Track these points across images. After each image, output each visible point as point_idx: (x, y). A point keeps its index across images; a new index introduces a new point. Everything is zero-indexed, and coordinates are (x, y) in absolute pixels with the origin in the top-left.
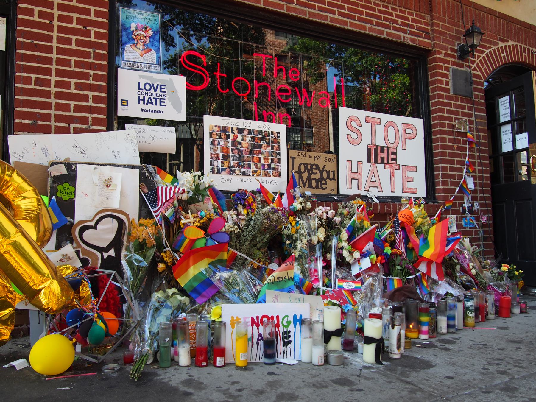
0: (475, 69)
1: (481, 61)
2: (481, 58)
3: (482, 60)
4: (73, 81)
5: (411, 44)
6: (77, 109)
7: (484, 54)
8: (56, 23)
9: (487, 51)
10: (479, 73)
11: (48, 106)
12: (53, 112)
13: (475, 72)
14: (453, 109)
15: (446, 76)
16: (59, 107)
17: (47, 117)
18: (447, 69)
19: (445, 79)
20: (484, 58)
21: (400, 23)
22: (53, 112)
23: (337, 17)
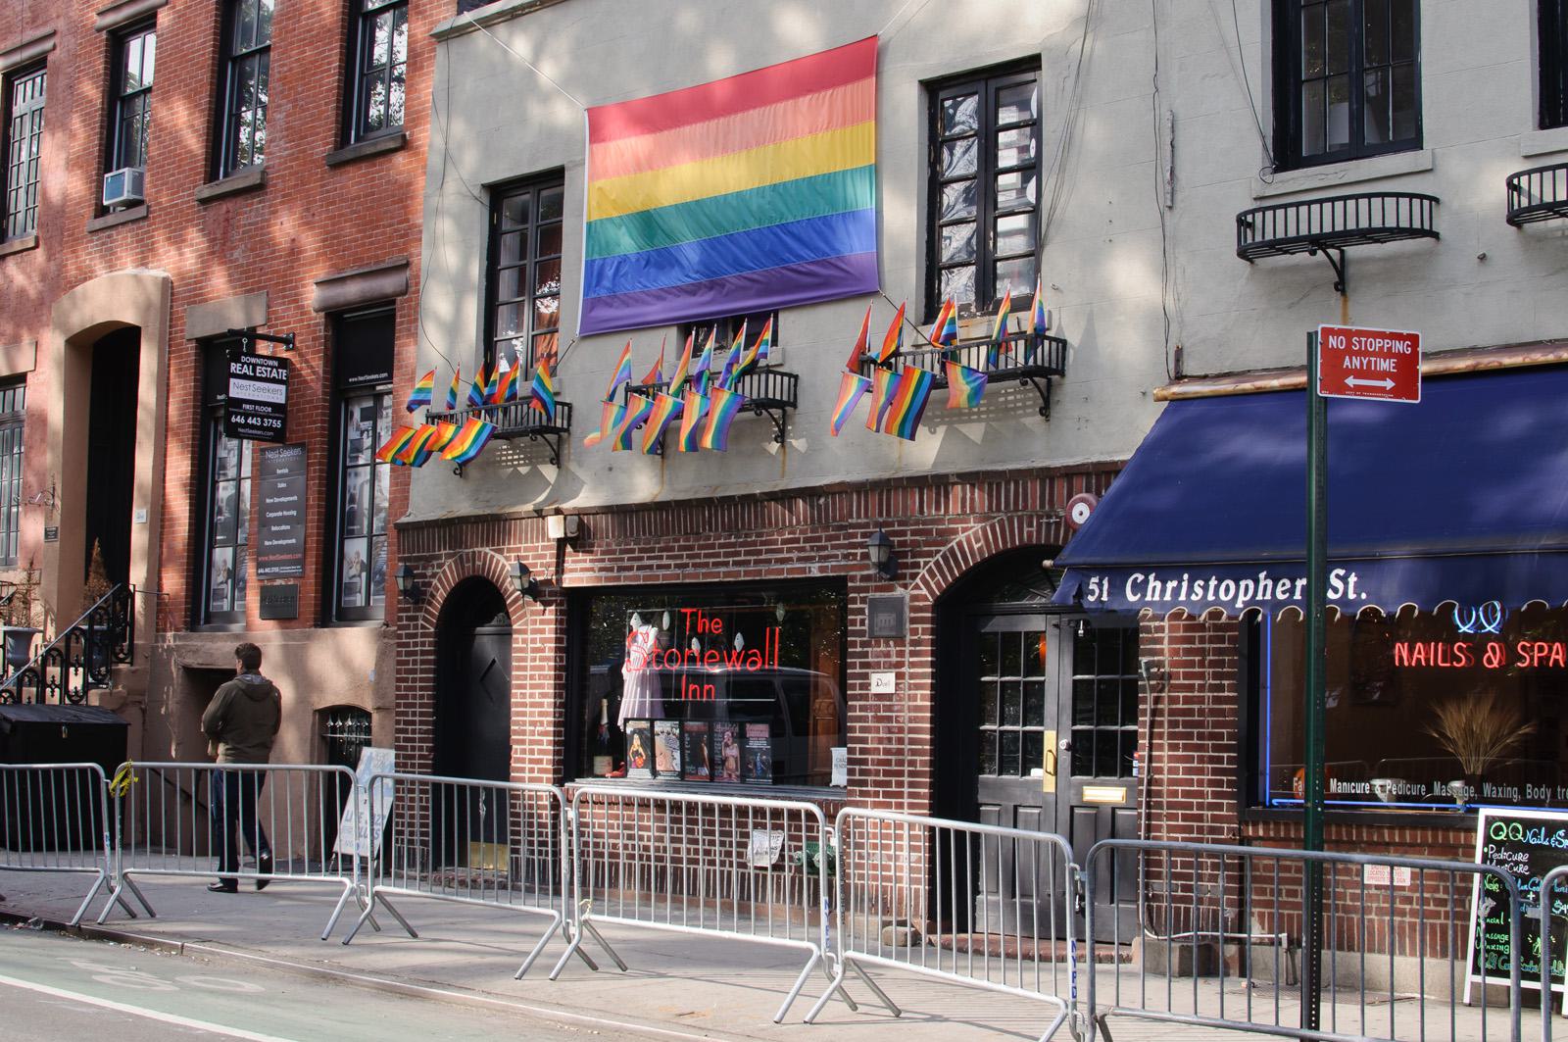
1: (930, 571)
2: (931, 564)
3: (934, 567)
4: (537, 691)
5: (819, 575)
7: (938, 557)
8: (530, 646)
9: (943, 549)
10: (924, 591)
13: (916, 592)
14: (870, 660)
15: (861, 611)
16: (532, 714)
18: (863, 601)
19: (859, 617)
20: (937, 563)
21: (808, 548)
22: (527, 719)
23: (732, 568)
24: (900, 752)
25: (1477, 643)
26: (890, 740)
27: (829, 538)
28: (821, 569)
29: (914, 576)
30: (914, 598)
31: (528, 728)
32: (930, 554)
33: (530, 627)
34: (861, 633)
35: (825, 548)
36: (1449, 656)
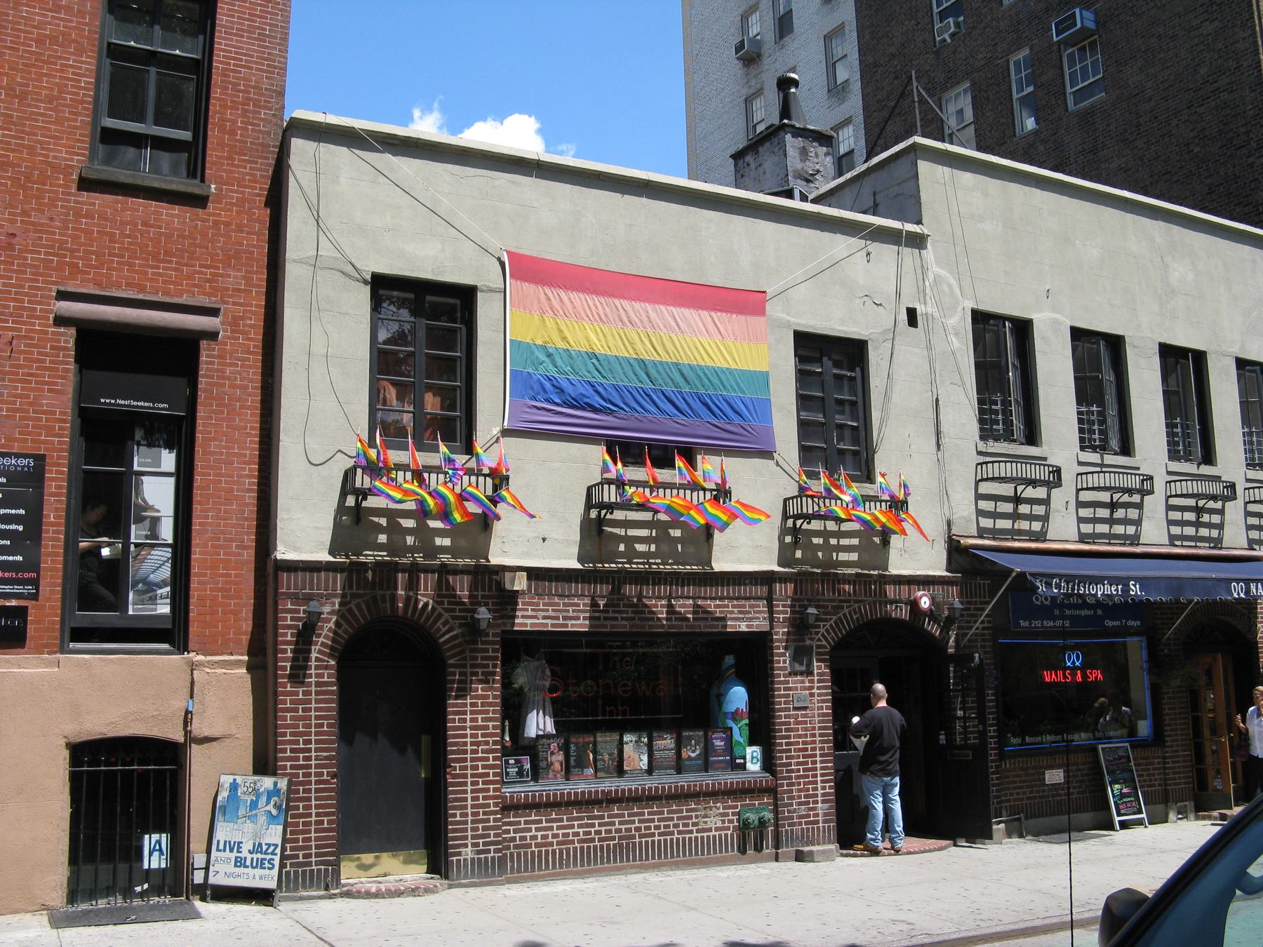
0: (819, 640)
1: (827, 630)
4: (480, 717)
6: (483, 735)
11: (465, 736)
12: (468, 740)
15: (783, 655)
17: (465, 744)
22: (468, 740)
24: (814, 742)
25: (1074, 668)
26: (806, 736)
27: (751, 606)
28: (748, 626)
29: (817, 633)
30: (818, 647)
31: (469, 748)
32: (826, 620)
33: (469, 662)
34: (784, 669)
35: (749, 612)
36: (1065, 677)
